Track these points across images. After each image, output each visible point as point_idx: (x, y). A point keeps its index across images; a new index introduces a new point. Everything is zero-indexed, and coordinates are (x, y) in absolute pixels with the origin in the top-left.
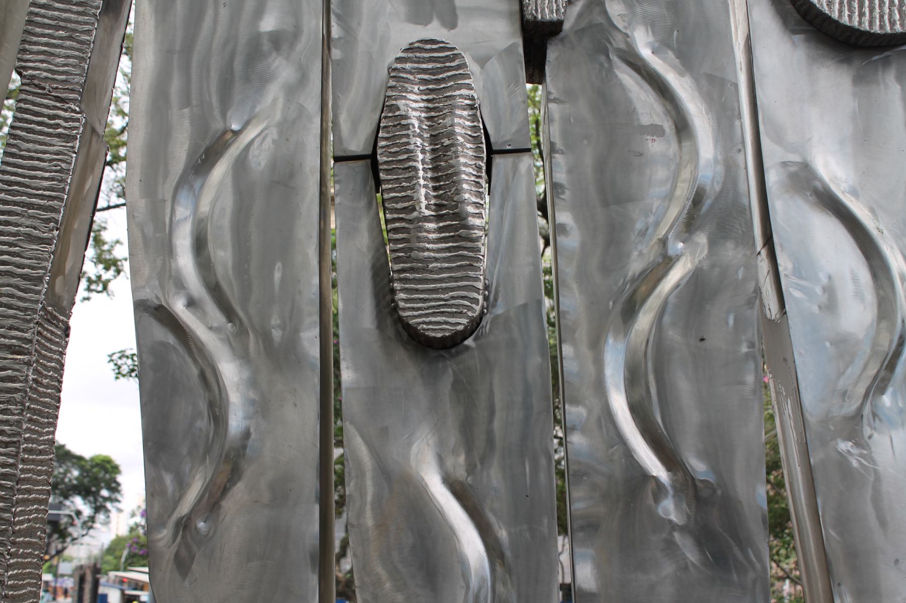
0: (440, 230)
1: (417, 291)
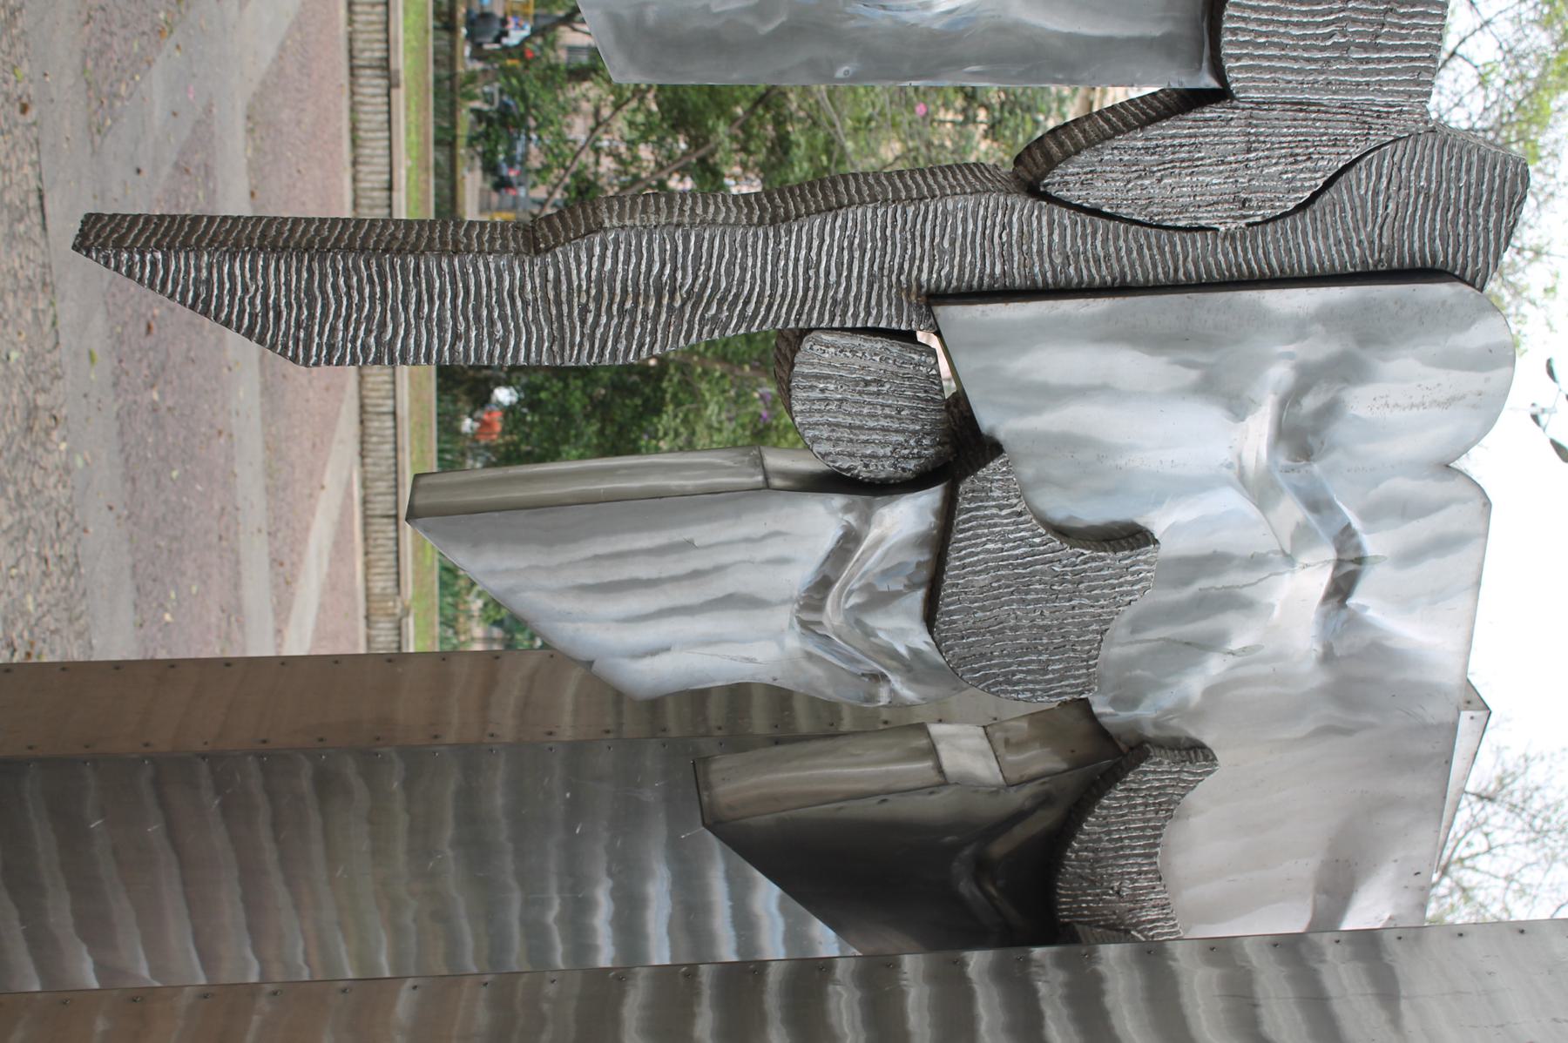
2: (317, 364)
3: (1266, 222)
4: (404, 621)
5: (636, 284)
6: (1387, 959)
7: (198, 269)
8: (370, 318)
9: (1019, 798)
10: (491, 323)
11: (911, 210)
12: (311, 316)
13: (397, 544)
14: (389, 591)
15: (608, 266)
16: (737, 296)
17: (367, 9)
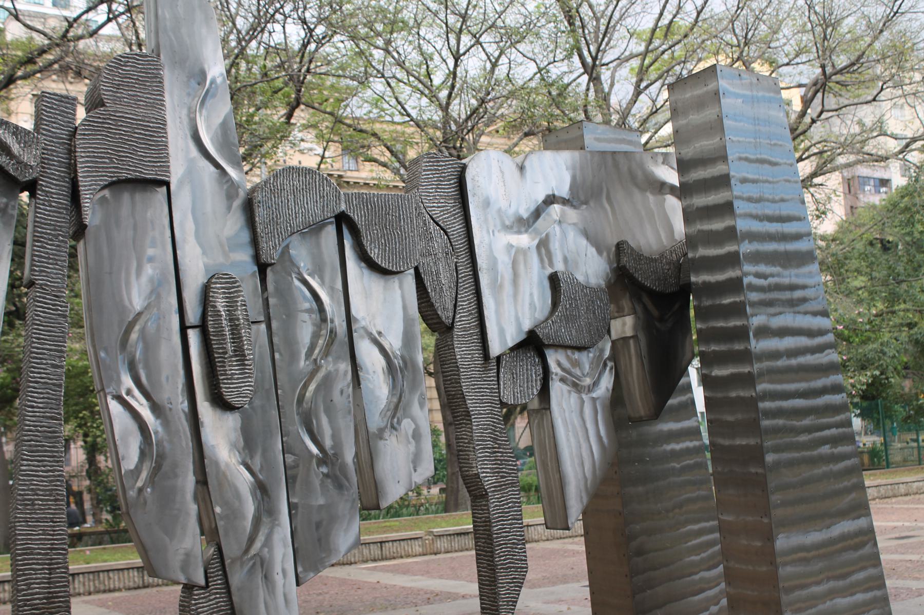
0: (237, 361)
1: (230, 388)
2: (527, 564)
3: (451, 245)
4: (436, 534)
5: (494, 460)
6: (691, 182)
7: (504, 605)
8: (512, 548)
9: (639, 309)
10: (509, 508)
11: (462, 370)
12: (513, 567)
13: (395, 541)
14: (420, 543)
15: (488, 470)
16: (493, 426)
17: (111, 582)
